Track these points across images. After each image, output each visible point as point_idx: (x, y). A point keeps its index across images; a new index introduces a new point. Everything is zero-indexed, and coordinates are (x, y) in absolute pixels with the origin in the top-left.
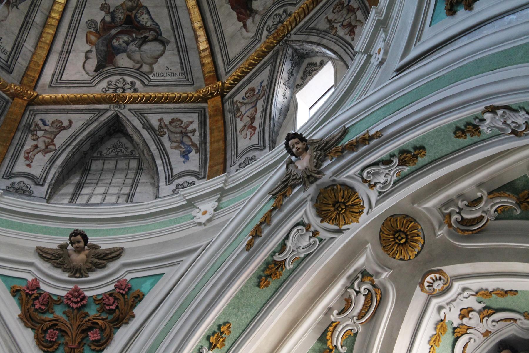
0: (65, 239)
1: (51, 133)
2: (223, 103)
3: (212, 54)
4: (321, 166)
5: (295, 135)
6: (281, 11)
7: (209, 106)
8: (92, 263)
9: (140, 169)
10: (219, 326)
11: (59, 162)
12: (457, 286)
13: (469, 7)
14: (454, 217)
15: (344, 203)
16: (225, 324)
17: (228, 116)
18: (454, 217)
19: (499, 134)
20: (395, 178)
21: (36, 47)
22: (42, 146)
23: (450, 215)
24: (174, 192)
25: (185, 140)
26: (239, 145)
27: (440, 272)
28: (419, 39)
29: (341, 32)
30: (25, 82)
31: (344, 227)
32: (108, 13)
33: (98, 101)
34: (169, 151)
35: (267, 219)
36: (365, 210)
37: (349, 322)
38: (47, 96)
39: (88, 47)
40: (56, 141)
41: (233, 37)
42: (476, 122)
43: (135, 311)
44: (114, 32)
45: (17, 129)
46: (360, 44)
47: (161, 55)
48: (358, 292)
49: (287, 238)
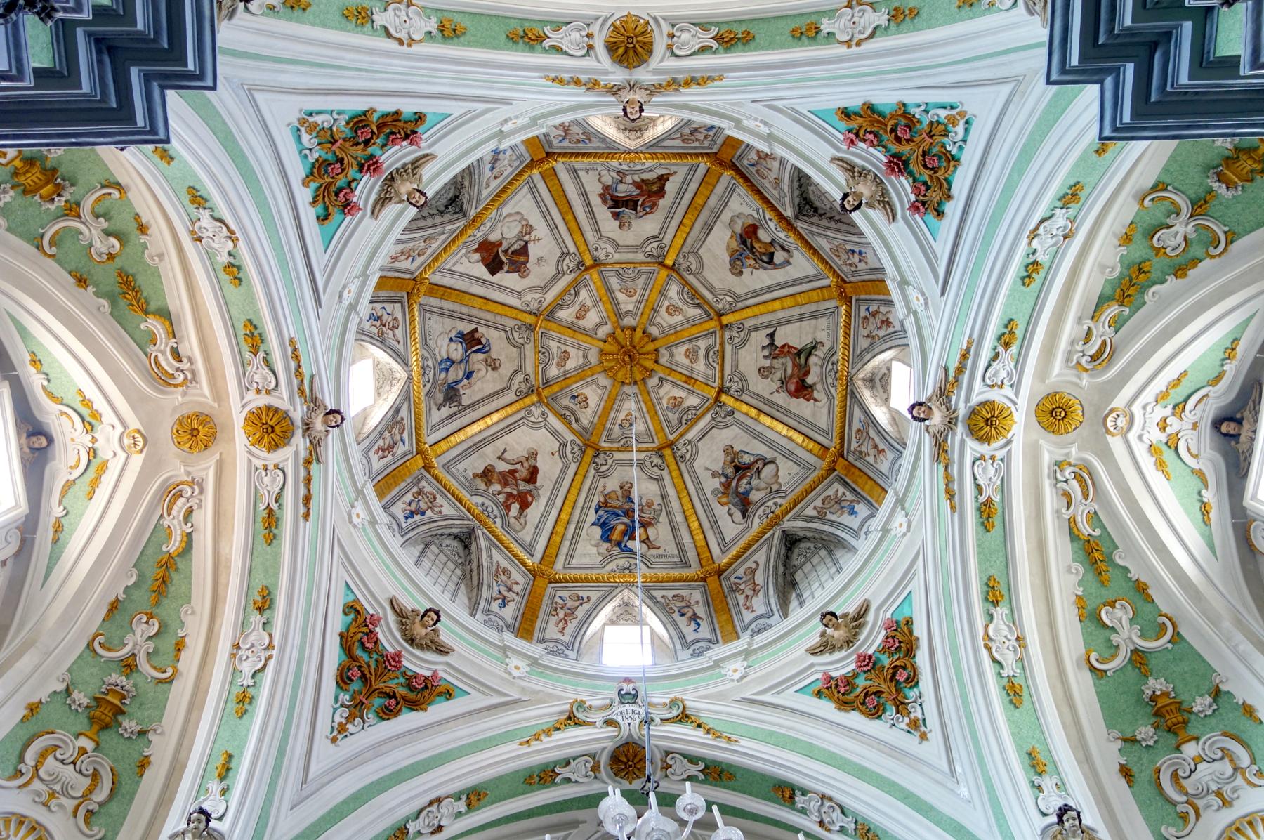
1: (749, 580)
4: (951, 406)
6: (830, 366)
9: (830, 552)
10: (987, 585)
13: (949, 197)
15: (993, 417)
16: (989, 579)
17: (858, 464)
20: (1012, 364)
21: (692, 536)
22: (750, 593)
25: (843, 504)
26: (883, 471)
28: (936, 258)
29: (882, 333)
30: (704, 564)
31: (1009, 436)
35: (948, 479)
36: (1013, 409)
39: (726, 508)
40: (757, 582)
41: (814, 415)
42: (1032, 259)
43: (916, 633)
44: (734, 484)
45: (726, 597)
49: (975, 479)
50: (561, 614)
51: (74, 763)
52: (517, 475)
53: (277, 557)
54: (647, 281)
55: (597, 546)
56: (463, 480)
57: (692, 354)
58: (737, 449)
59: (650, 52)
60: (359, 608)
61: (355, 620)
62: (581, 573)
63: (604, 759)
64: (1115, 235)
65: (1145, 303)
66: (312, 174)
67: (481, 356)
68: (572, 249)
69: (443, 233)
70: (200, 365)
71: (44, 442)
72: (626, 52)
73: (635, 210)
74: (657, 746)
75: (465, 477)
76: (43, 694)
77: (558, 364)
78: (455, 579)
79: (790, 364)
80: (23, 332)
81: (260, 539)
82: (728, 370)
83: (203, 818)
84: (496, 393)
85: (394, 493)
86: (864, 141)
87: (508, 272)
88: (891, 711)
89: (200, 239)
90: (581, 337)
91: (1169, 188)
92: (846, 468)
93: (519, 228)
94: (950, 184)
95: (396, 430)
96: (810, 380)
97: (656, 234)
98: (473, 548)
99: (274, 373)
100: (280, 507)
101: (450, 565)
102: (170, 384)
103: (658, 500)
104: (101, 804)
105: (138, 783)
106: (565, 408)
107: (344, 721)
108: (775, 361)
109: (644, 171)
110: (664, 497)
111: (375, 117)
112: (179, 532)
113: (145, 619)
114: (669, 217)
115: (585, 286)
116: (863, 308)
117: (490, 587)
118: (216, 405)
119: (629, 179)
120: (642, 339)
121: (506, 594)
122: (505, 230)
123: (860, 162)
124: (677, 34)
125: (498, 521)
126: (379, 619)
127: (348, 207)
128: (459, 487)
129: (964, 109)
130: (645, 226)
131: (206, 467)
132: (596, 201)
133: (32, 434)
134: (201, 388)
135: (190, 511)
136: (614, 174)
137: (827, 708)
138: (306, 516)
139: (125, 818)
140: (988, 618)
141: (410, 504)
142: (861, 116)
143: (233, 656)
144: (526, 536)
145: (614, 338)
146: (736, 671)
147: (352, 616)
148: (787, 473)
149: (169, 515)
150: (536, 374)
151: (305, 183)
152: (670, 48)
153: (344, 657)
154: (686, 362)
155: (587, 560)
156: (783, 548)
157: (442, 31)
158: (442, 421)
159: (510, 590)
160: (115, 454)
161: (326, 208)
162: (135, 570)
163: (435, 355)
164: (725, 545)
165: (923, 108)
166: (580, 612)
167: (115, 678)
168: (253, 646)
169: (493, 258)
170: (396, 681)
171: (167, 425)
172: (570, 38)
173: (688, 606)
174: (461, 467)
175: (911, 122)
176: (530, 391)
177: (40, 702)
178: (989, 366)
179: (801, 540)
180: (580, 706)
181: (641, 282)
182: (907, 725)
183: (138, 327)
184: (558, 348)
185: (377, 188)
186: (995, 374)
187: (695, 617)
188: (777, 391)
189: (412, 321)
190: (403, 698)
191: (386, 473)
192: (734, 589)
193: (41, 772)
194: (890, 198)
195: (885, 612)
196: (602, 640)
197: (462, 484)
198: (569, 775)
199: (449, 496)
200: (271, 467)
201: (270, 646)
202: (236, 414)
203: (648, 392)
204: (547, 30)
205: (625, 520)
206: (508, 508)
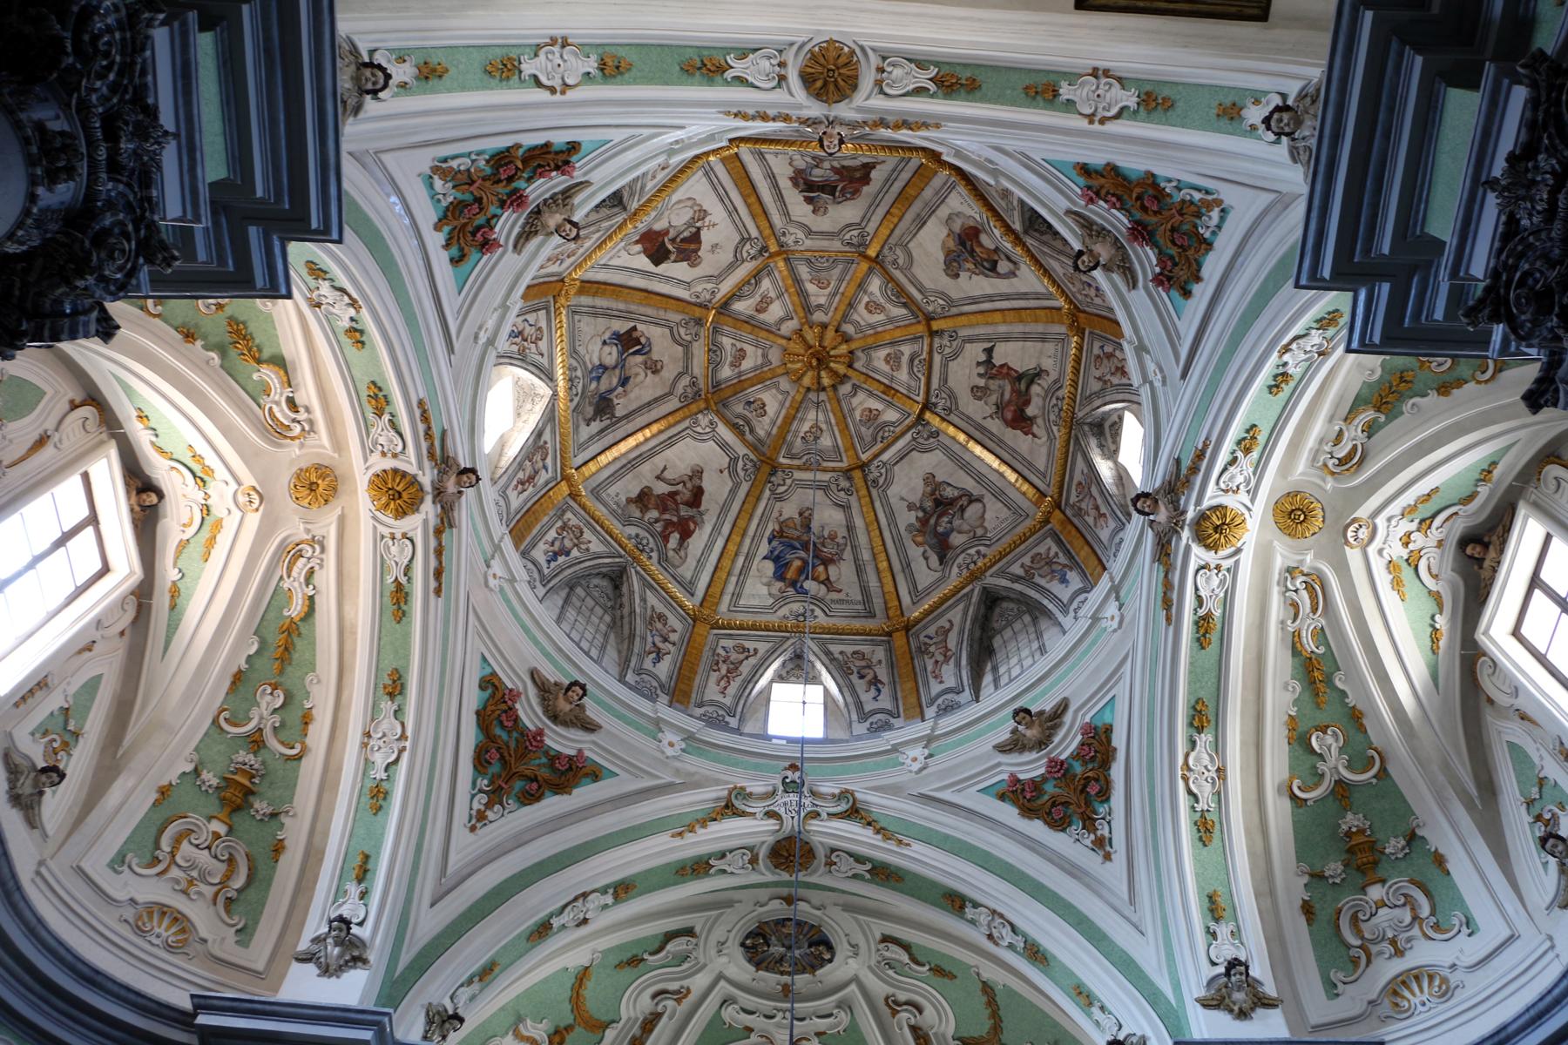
0: (1012, 724)
2: (1064, 513)
5: (1138, 497)
6: (1054, 401)
7: (1055, 523)
8: (1048, 728)
9: (1035, 620)
10: (1194, 708)
11: (964, 662)
12: (1380, 521)
13: (1198, 279)
14: (1330, 463)
15: (1224, 524)
16: (1197, 702)
17: (1075, 520)
18: (1330, 463)
20: (1251, 470)
21: (880, 580)
22: (940, 658)
24: (1076, 618)
25: (1055, 567)
27: (1354, 520)
28: (1179, 338)
29: (1115, 380)
32: (917, 509)
34: (1047, 586)
35: (1168, 585)
37: (1309, 621)
39: (921, 549)
40: (949, 646)
42: (1281, 370)
43: (1115, 743)
44: (932, 521)
45: (912, 659)
46: (1135, 379)
47: (984, 511)
48: (1296, 591)
49: (1197, 589)
51: (209, 848)
52: (678, 498)
53: (407, 636)
54: (844, 272)
55: (768, 585)
56: (615, 507)
58: (939, 478)
59: (855, 87)
61: (493, 696)
62: (749, 619)
63: (763, 853)
66: (445, 217)
67: (639, 359)
68: (754, 233)
70: (318, 414)
72: (825, 84)
73: (833, 195)
74: (821, 843)
75: (617, 504)
76: (172, 776)
77: (732, 365)
78: (603, 627)
79: (1008, 388)
80: (127, 389)
82: (935, 383)
83: (344, 926)
84: (656, 400)
86: (1106, 201)
87: (675, 261)
88: (1076, 827)
89: (319, 305)
92: (1062, 523)
95: (538, 457)
96: (1030, 411)
97: (858, 221)
98: (625, 589)
99: (401, 435)
100: (409, 580)
101: (598, 610)
102: (286, 437)
103: (842, 532)
104: (239, 891)
105: (274, 869)
106: (738, 416)
107: (482, 808)
108: (991, 381)
110: (850, 528)
111: (521, 152)
112: (300, 595)
113: (269, 691)
114: (873, 205)
115: (769, 274)
116: (1097, 345)
117: (644, 639)
118: (336, 455)
119: (826, 165)
121: (660, 645)
123: (1100, 221)
124: (889, 69)
125: (655, 555)
126: (519, 694)
127: (487, 245)
128: (611, 517)
129: (1221, 197)
130: (845, 213)
131: (328, 525)
132: (785, 184)
133: (140, 491)
134: (320, 439)
135: (311, 573)
136: (809, 160)
137: (1008, 813)
138: (438, 592)
139: (263, 905)
140: (1190, 746)
141: (552, 544)
142: (1103, 176)
143: (364, 745)
144: (686, 571)
145: (801, 336)
146: (915, 760)
147: (489, 691)
148: (995, 513)
149: (289, 577)
151: (438, 227)
152: (879, 83)
153: (481, 737)
154: (886, 368)
155: (755, 602)
156: (982, 606)
157: (602, 70)
158: (591, 438)
159: (665, 640)
160: (229, 512)
161: (461, 249)
163: (585, 363)
164: (917, 595)
165: (1174, 184)
166: (745, 669)
167: (243, 756)
168: (384, 735)
169: (657, 248)
170: (537, 762)
171: (285, 478)
172: (757, 68)
173: (869, 667)
174: (612, 490)
177: (171, 784)
178: (1225, 470)
179: (1004, 599)
181: (836, 272)
182: (1092, 842)
183: (250, 377)
184: (733, 345)
185: (522, 221)
186: (1232, 478)
187: (875, 682)
188: (991, 416)
190: (545, 781)
192: (923, 650)
193: (178, 859)
195: (1084, 715)
196: (768, 700)
197: (613, 512)
199: (598, 528)
200: (398, 536)
201: (403, 737)
202: (360, 470)
203: (839, 401)
205: (802, 554)
206: (666, 539)
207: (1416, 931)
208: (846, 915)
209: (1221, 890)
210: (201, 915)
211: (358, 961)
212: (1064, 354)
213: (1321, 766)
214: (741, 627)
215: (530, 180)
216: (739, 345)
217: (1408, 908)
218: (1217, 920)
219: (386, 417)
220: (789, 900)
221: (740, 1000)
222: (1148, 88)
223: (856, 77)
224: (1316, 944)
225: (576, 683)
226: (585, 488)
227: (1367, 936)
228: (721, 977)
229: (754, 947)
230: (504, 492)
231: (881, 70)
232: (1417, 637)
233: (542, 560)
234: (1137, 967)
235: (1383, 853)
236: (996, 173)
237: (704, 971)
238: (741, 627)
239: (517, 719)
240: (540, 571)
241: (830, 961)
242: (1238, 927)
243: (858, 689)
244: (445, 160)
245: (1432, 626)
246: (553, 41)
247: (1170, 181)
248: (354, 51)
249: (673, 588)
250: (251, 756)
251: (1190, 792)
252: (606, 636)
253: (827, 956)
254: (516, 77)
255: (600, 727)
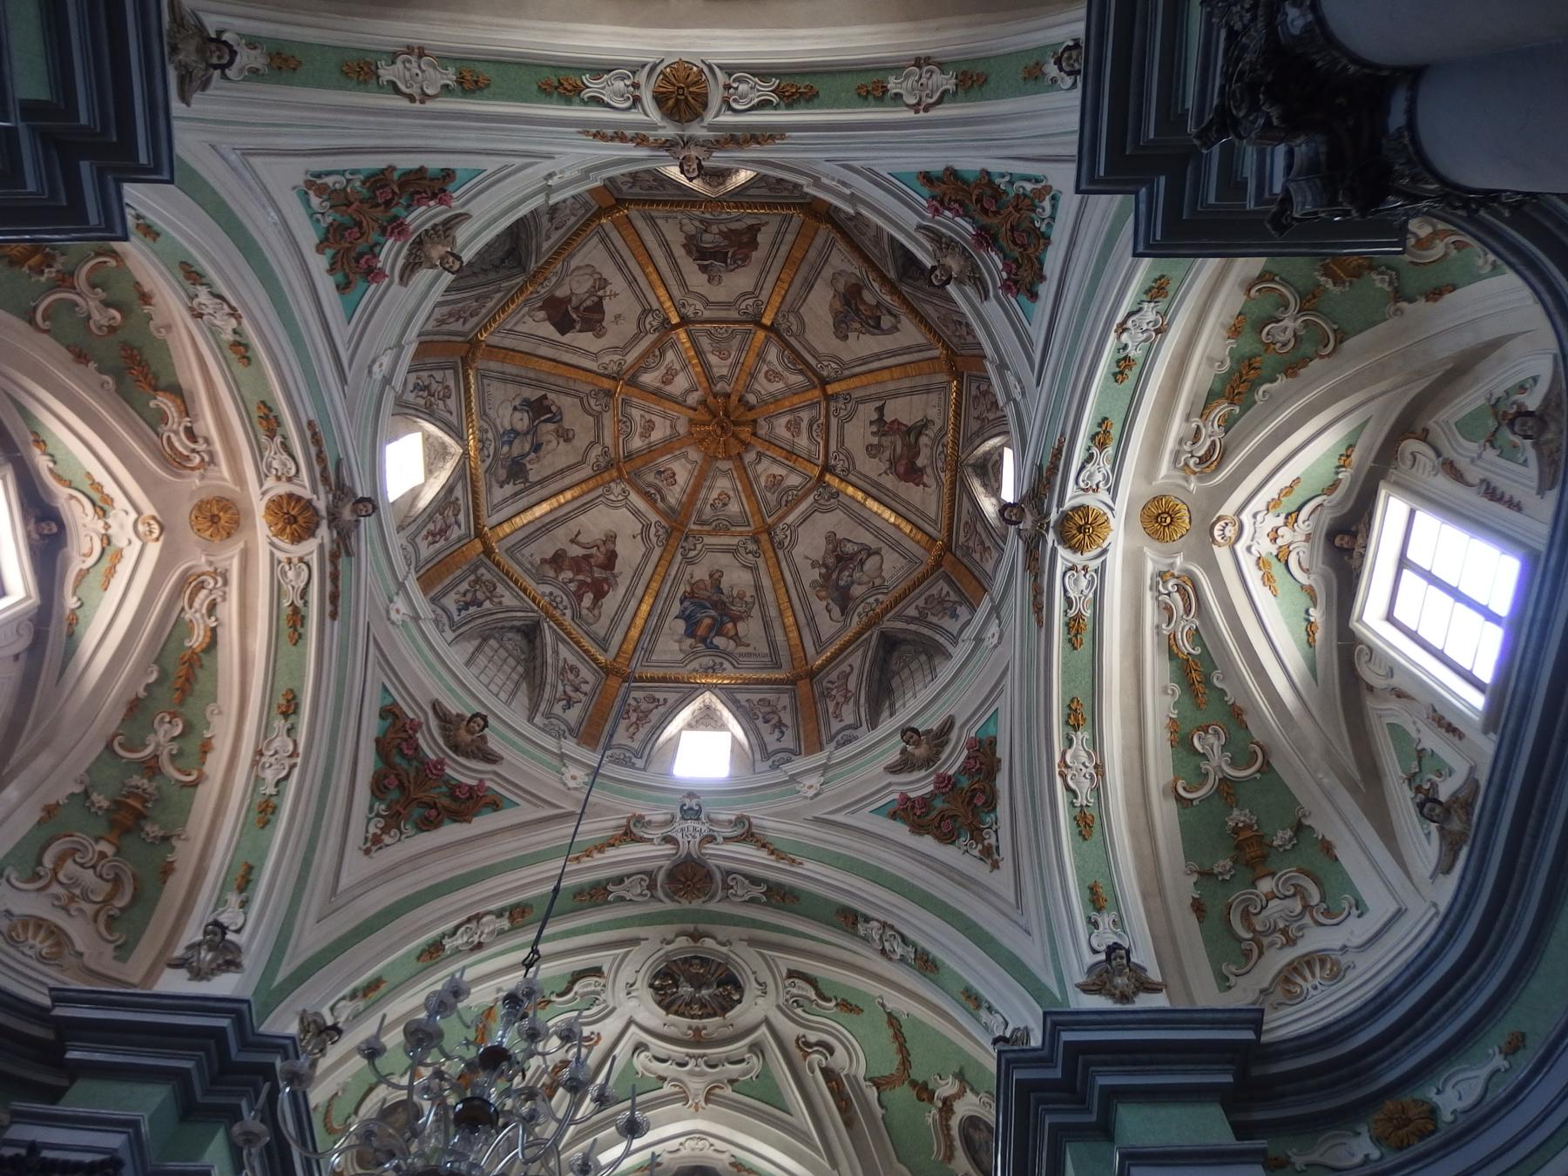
3: (918, 528)
6: (940, 448)
7: (946, 568)
9: (930, 658)
10: (1069, 706)
11: (862, 700)
14: (1192, 462)
15: (1087, 523)
16: (1072, 701)
17: (965, 561)
18: (1192, 462)
19: (1151, 352)
20: (1108, 467)
21: (786, 634)
22: (841, 700)
23: (1186, 464)
25: (946, 605)
29: (991, 416)
30: (796, 664)
32: (820, 566)
33: (859, 634)
34: (939, 623)
35: (1037, 591)
38: (820, 662)
42: (1122, 355)
44: (834, 576)
45: (815, 703)
48: (1169, 594)
49: (1065, 591)
50: (634, 717)
51: (94, 867)
53: (303, 656)
54: (743, 342)
55: (680, 641)
57: (794, 426)
59: (705, 106)
60: (397, 712)
61: (393, 725)
62: (660, 673)
63: (660, 878)
64: (1223, 325)
65: (1255, 402)
67: (551, 427)
69: (499, 291)
70: (218, 446)
71: (55, 529)
72: (677, 101)
73: (726, 263)
74: (718, 867)
76: (60, 796)
77: (642, 435)
78: (515, 676)
79: (899, 443)
81: (285, 638)
82: (833, 447)
83: (218, 930)
84: (569, 468)
85: (446, 582)
86: (950, 210)
87: (580, 331)
89: (200, 316)
90: (668, 404)
91: (1277, 278)
93: (590, 283)
94: (1041, 264)
96: (920, 462)
97: (751, 289)
98: (538, 641)
99: (293, 458)
100: (306, 603)
101: (511, 661)
102: (185, 467)
103: (750, 592)
104: (122, 910)
105: (160, 890)
106: (650, 485)
107: (379, 832)
109: (731, 220)
110: (758, 588)
111: (396, 175)
112: (202, 627)
113: (167, 719)
114: (764, 272)
115: (672, 346)
116: (974, 386)
117: (555, 687)
118: (238, 489)
119: (714, 229)
120: (736, 408)
121: (572, 694)
122: (575, 285)
125: (568, 612)
126: (420, 725)
127: (372, 274)
129: (1050, 183)
130: (739, 281)
132: (679, 252)
134: (220, 471)
135: (212, 608)
137: (900, 831)
138: (334, 616)
140: (1067, 743)
144: (600, 628)
147: (389, 721)
149: (191, 607)
150: (616, 446)
151: (320, 249)
153: (380, 765)
154: (788, 435)
155: (667, 657)
157: (461, 84)
158: (505, 500)
159: (577, 690)
160: (130, 542)
161: (346, 276)
162: (155, 668)
163: (495, 426)
165: (1007, 179)
166: (655, 716)
168: (276, 753)
169: (562, 315)
170: (438, 790)
171: (187, 508)
174: (527, 551)
175: (997, 193)
176: (609, 466)
177: (58, 804)
178: (1082, 468)
179: (904, 641)
180: (638, 821)
181: (735, 342)
184: (642, 416)
185: (405, 252)
186: (1090, 476)
187: (780, 725)
188: (886, 472)
189: (467, 390)
190: (446, 808)
191: (437, 560)
192: (826, 695)
193: (61, 876)
194: (981, 274)
195: (969, 730)
197: (526, 571)
198: (622, 893)
199: (512, 584)
200: (295, 560)
203: (745, 468)
204: (586, 78)
205: (713, 613)
206: (580, 598)
207: (1307, 920)
208: (751, 950)
209: (1102, 882)
210: (78, 931)
211: (232, 964)
212: (947, 403)
213: (1204, 766)
214: (652, 680)
215: (409, 207)
216: (648, 416)
217: (1298, 897)
218: (1099, 910)
219: (278, 439)
220: (696, 936)
221: (651, 1046)
222: (964, 67)
223: (706, 95)
224: (1208, 941)
225: (477, 715)
226: (500, 548)
227: (1258, 928)
228: (631, 1022)
229: (662, 988)
230: (413, 540)
231: (727, 87)
232: (1293, 633)
233: (453, 608)
234: (1024, 966)
235: (1271, 846)
236: (853, 199)
237: (615, 1014)
238: (652, 680)
239: (417, 748)
240: (450, 618)
241: (739, 1001)
242: (1121, 917)
243: (762, 731)
244: (319, 176)
245: (1308, 620)
246: (410, 50)
247: (1002, 175)
248: (201, 28)
249: (587, 642)
250: (145, 781)
251: (1068, 788)
252: (517, 685)
253: (736, 997)
254: (374, 81)
255: (502, 758)
